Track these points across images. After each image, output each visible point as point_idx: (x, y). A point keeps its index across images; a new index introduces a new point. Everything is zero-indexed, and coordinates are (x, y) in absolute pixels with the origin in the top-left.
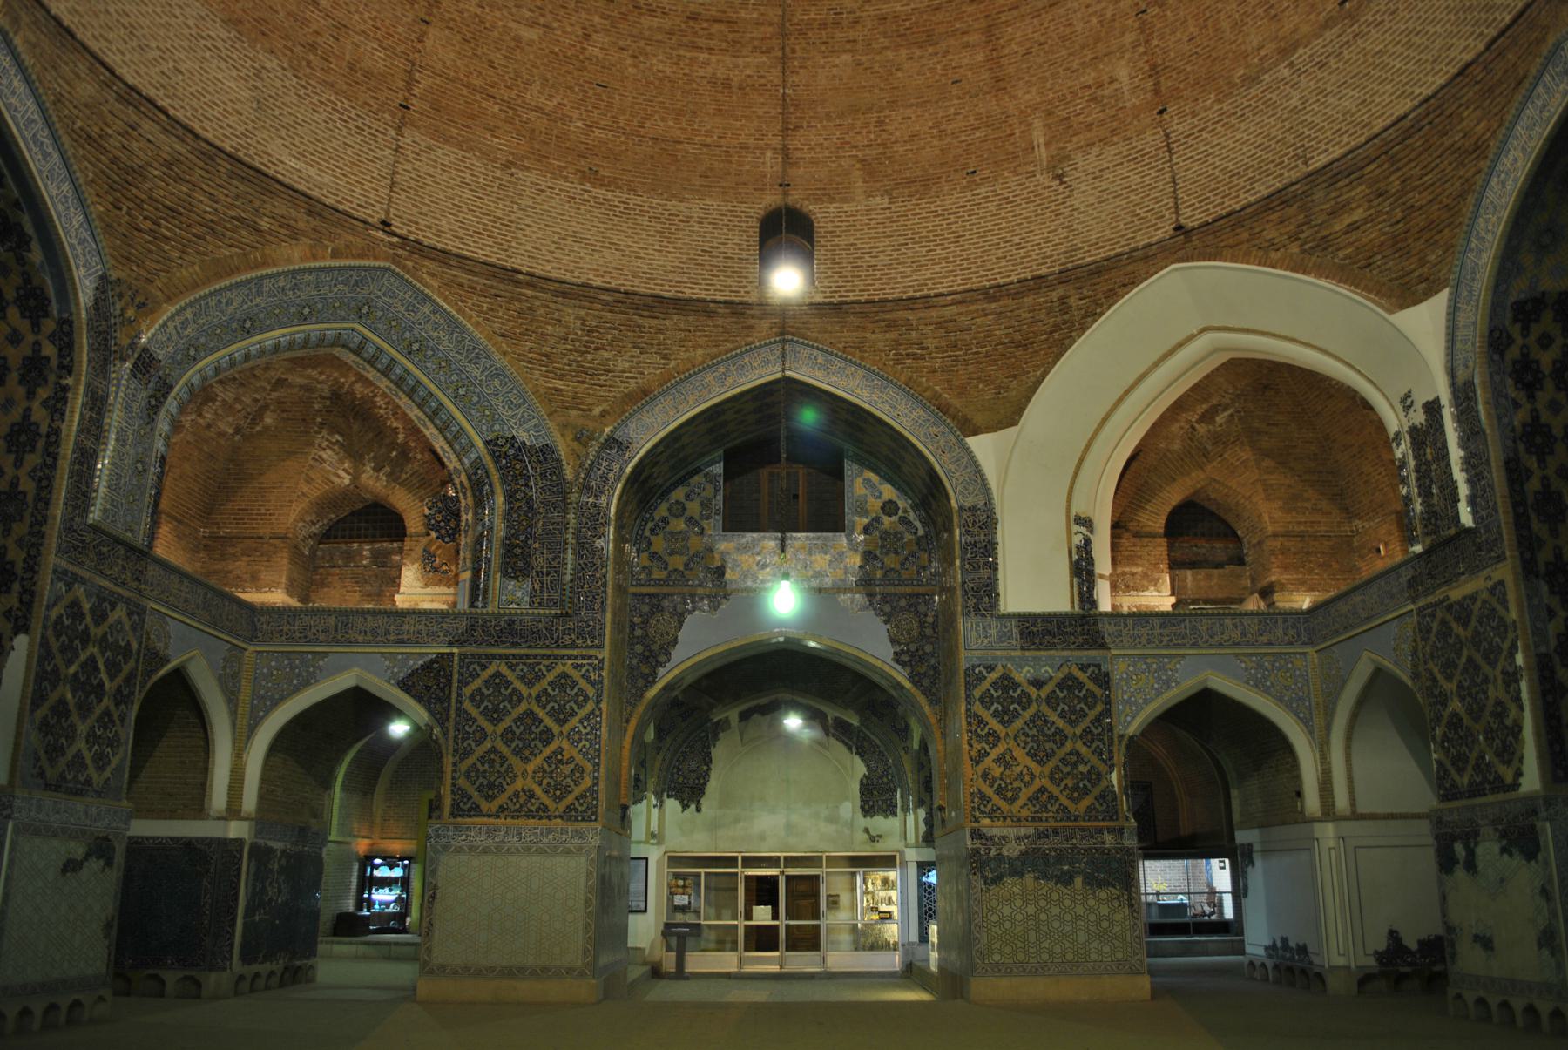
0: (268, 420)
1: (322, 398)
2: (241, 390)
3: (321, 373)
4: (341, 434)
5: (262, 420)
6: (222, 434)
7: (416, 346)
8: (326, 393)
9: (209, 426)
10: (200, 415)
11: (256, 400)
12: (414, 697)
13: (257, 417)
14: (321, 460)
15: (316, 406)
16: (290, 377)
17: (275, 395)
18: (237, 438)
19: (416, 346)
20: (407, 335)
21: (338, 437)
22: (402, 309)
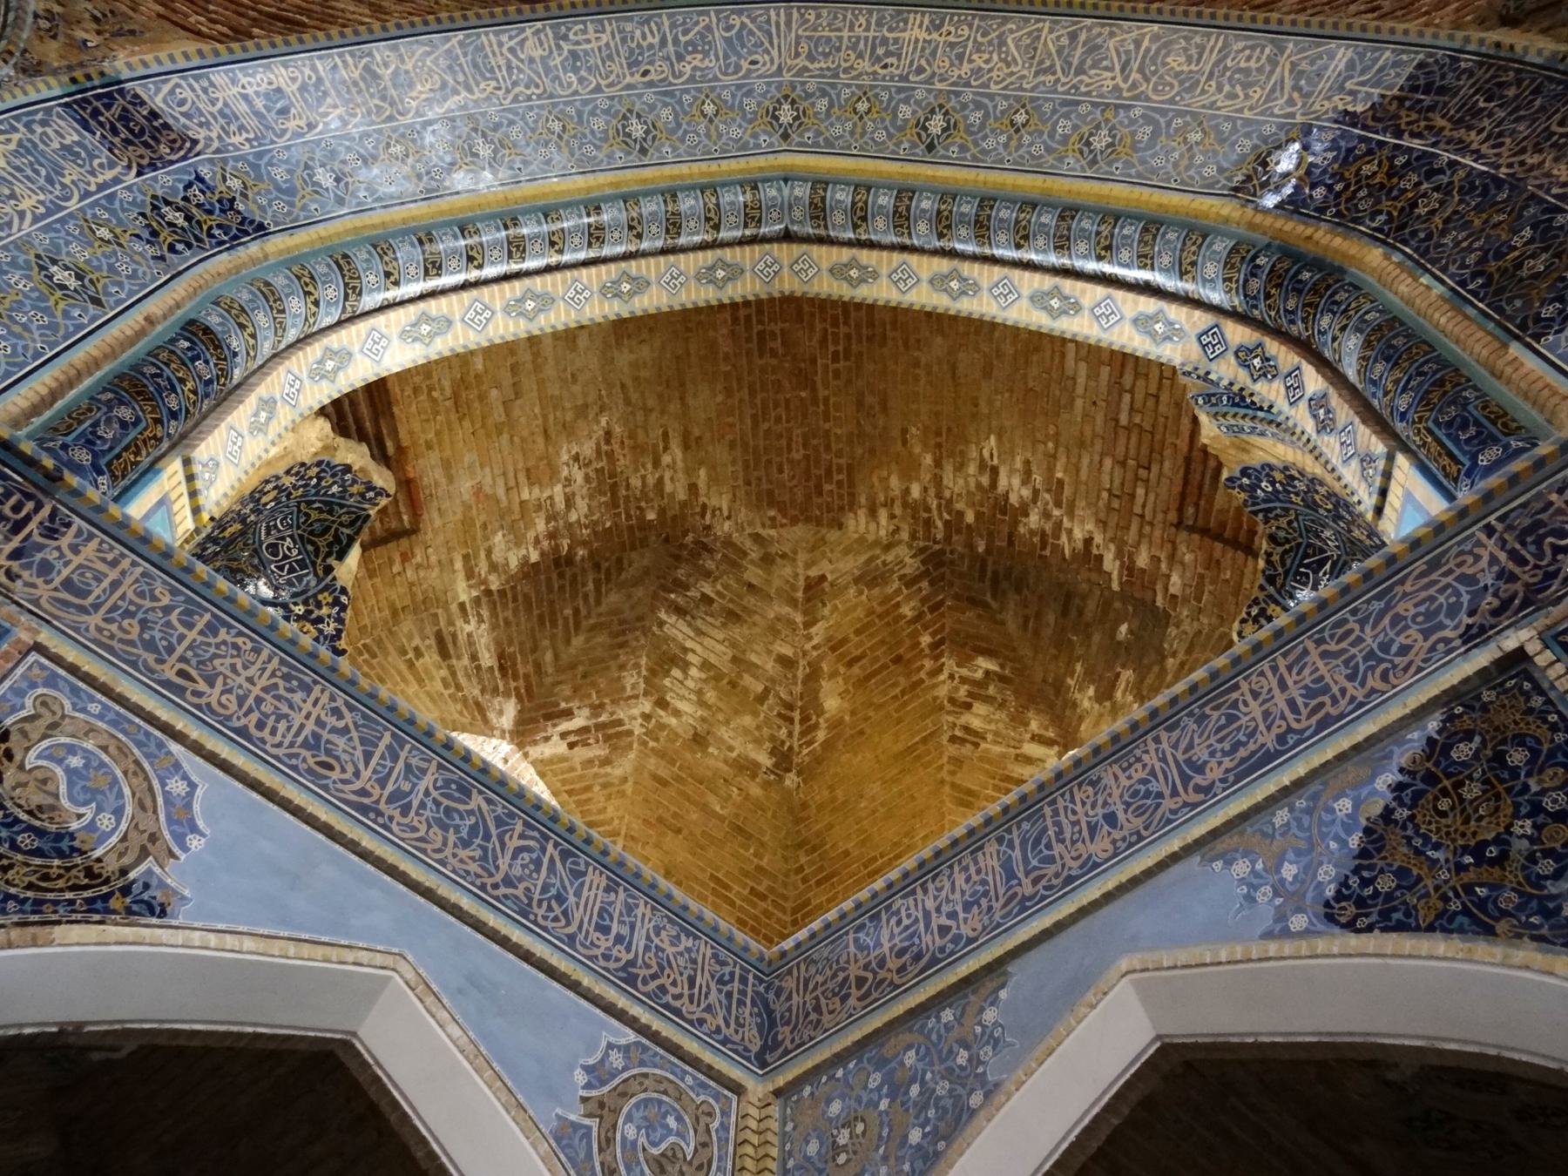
0: (831, 703)
1: (910, 582)
2: (738, 632)
3: (873, 513)
4: (988, 653)
5: (820, 711)
6: (747, 767)
7: (936, 125)
8: (912, 565)
9: (699, 741)
10: (662, 703)
11: (786, 662)
12: (1442, 924)
13: (804, 710)
14: (973, 737)
15: (907, 610)
16: (824, 568)
17: (818, 631)
18: (791, 780)
19: (936, 125)
20: (905, 111)
21: (985, 664)
22: (865, 65)
